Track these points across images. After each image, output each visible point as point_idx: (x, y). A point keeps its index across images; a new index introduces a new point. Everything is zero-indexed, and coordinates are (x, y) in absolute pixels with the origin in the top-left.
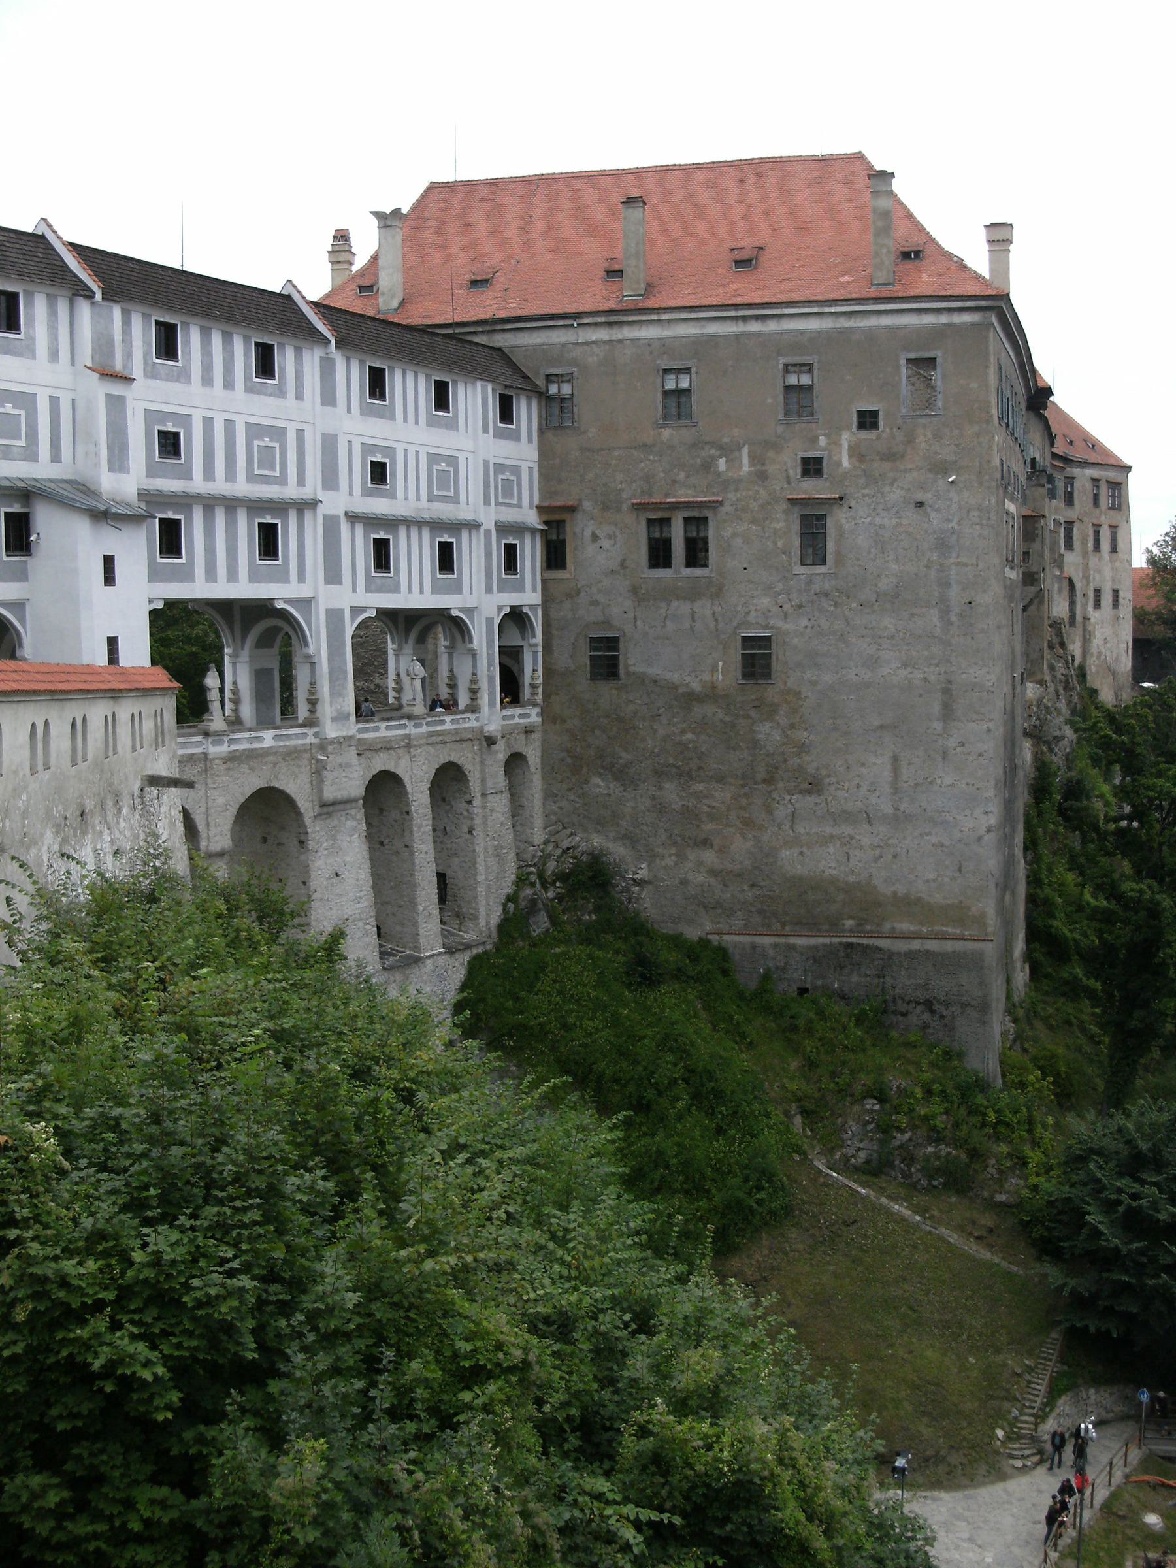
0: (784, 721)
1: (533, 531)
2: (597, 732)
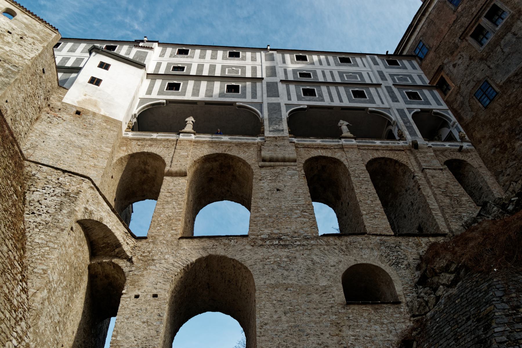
2: (503, 124)
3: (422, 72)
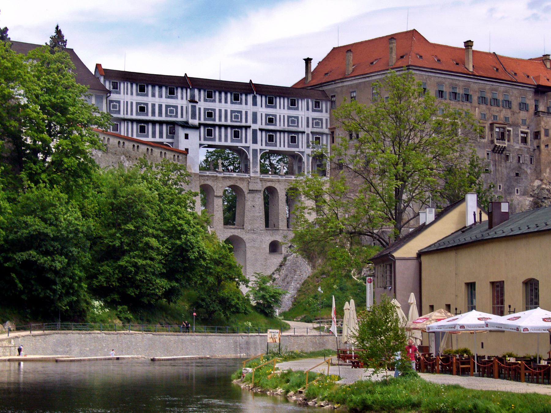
1: (327, 134)
3: (329, 116)
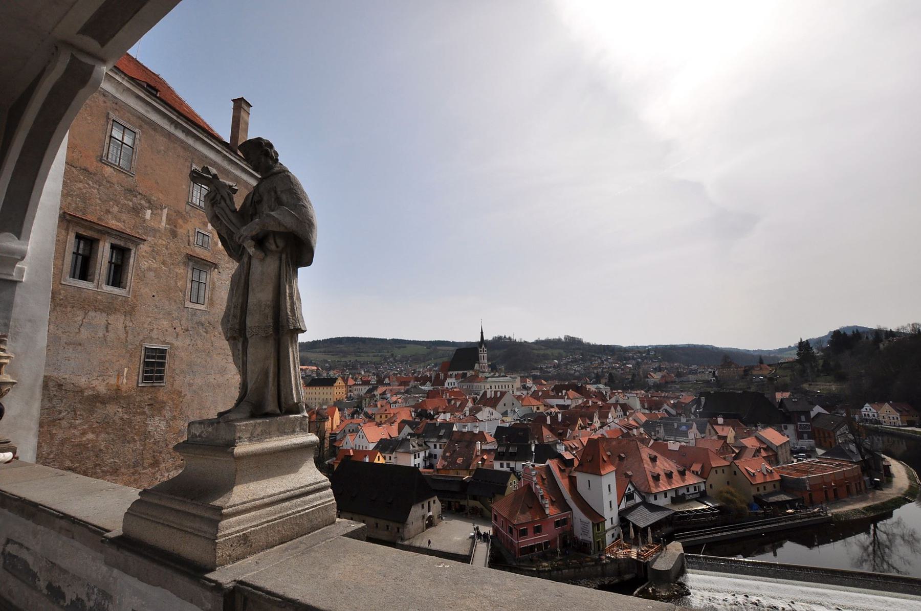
0: (168, 415)
